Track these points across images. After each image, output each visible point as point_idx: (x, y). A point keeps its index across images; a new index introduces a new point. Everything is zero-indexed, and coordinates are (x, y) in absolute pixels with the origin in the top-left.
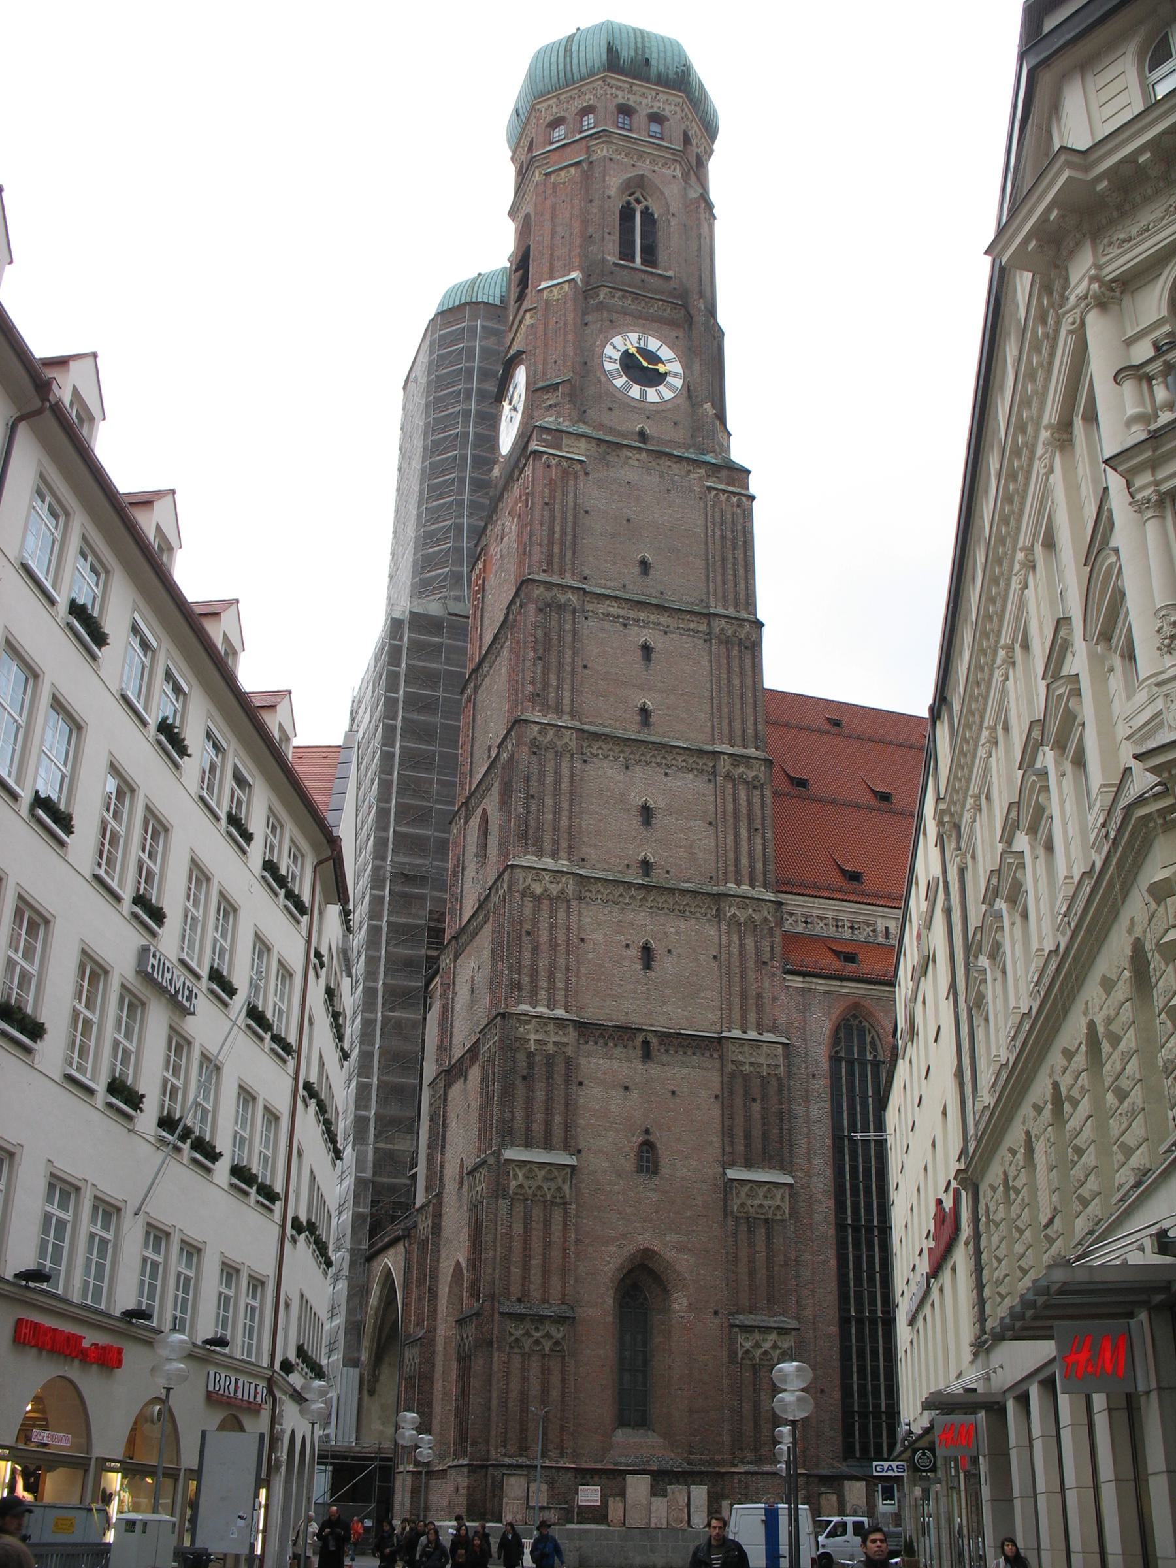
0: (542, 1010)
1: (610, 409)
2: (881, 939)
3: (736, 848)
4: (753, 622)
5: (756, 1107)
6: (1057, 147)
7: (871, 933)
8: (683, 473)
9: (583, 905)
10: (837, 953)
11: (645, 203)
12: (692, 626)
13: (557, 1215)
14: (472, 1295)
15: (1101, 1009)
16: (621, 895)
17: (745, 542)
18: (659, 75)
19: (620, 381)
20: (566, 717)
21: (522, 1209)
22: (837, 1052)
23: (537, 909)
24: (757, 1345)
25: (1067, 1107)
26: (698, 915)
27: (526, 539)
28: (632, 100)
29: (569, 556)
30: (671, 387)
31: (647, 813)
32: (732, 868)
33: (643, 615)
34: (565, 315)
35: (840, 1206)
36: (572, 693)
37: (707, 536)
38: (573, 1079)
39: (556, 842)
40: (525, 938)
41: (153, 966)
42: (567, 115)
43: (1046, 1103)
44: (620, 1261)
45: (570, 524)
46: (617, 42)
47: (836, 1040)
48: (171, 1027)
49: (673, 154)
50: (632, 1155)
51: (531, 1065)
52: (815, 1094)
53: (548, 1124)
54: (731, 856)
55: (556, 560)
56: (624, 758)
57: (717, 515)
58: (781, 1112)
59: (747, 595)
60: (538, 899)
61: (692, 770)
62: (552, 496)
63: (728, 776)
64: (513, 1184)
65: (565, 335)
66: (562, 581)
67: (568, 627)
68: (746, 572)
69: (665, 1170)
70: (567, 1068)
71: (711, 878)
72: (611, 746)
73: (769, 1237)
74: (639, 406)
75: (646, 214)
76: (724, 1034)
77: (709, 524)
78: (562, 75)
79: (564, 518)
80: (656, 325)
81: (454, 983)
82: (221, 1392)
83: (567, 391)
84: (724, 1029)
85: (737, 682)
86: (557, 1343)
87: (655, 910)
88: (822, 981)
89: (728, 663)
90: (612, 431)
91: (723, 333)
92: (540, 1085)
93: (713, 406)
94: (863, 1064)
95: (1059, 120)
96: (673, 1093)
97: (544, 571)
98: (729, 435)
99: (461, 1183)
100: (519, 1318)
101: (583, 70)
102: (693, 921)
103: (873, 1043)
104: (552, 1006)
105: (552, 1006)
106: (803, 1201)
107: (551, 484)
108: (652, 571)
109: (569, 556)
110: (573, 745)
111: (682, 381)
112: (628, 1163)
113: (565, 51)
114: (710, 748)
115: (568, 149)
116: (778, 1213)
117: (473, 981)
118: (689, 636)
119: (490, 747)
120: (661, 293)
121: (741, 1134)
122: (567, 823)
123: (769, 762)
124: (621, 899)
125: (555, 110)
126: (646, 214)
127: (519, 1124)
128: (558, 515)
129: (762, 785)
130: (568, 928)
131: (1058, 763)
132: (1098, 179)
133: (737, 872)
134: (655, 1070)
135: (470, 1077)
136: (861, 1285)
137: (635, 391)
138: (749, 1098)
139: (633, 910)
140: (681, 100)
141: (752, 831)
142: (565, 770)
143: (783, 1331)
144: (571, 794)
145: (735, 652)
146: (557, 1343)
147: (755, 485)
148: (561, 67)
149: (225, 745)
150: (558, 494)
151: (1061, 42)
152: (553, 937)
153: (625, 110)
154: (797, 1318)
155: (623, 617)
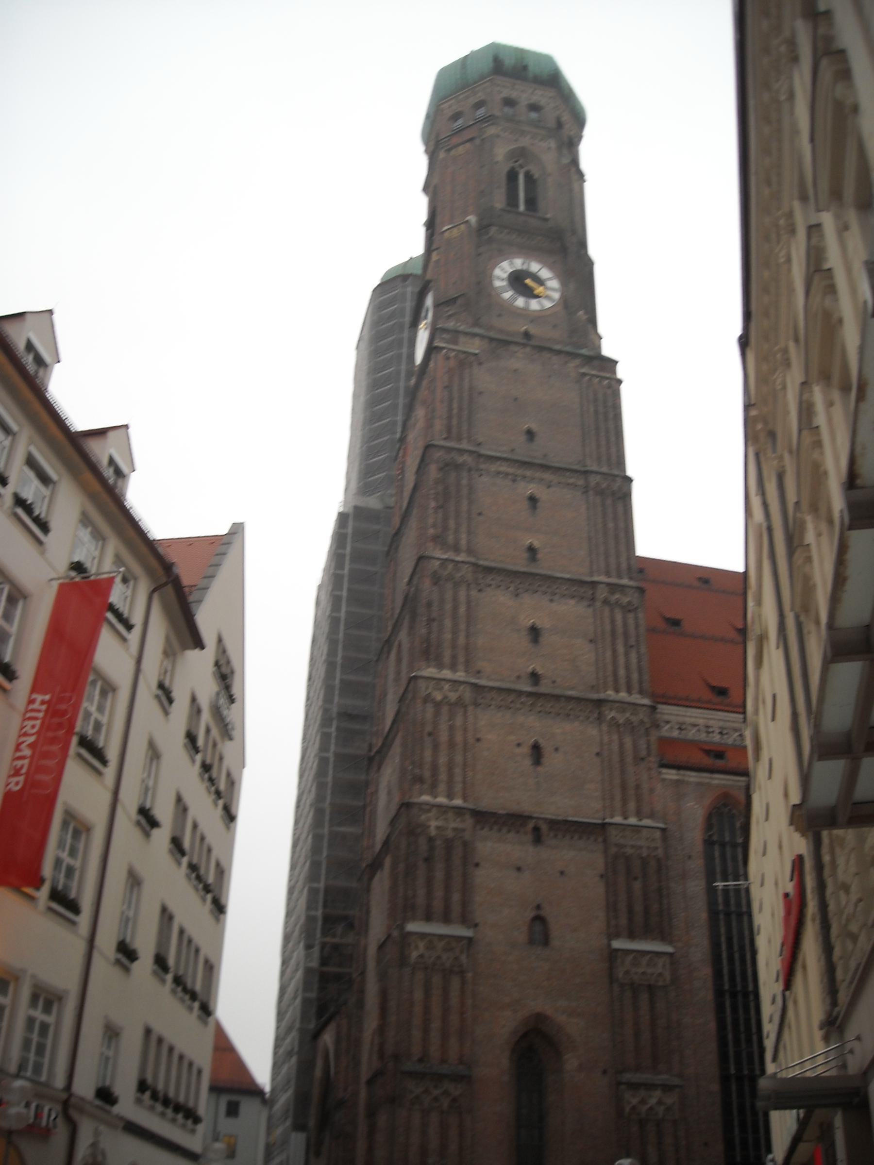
0: (442, 800)
5: (637, 885)
10: (708, 752)
12: (571, 481)
13: (455, 982)
19: (507, 295)
22: (710, 836)
23: (437, 714)
28: (514, 95)
31: (535, 633)
32: (610, 679)
35: (718, 974)
38: (469, 861)
39: (454, 657)
47: (709, 825)
51: (432, 848)
53: (447, 900)
60: (438, 705)
61: (573, 597)
63: (606, 602)
64: (414, 954)
66: (457, 446)
74: (524, 314)
75: (529, 177)
76: (607, 821)
85: (611, 525)
86: (454, 1100)
93: (586, 313)
97: (445, 439)
104: (450, 796)
114: (588, 579)
123: (641, 590)
124: (512, 705)
126: (529, 177)
127: (421, 900)
129: (636, 609)
130: (465, 730)
137: (520, 302)
141: (628, 647)
143: (667, 1088)
145: (609, 502)
146: (454, 1100)
153: (509, 102)
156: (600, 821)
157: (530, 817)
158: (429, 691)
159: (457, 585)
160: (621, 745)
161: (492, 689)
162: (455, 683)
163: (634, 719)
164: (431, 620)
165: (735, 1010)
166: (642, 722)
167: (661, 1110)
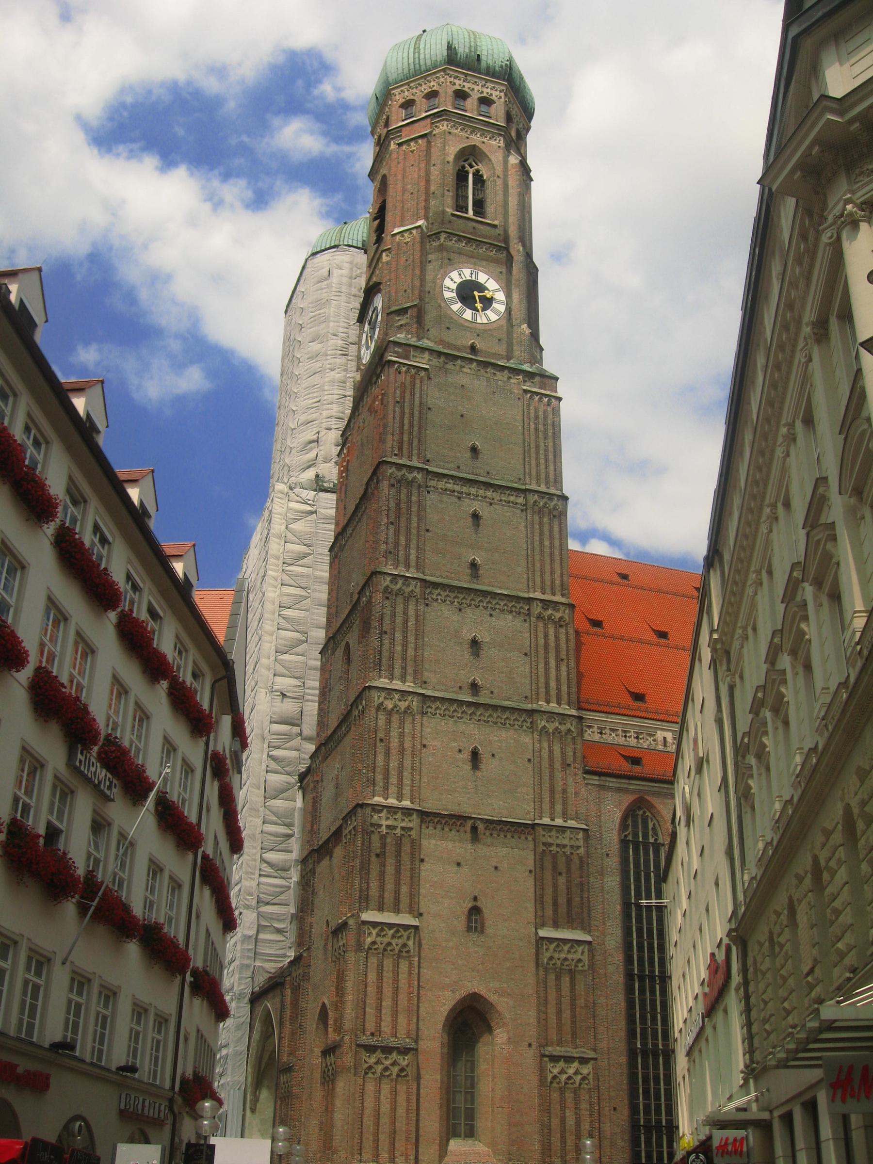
0: (392, 801)
1: (448, 328)
3: (546, 674)
4: (558, 496)
5: (562, 880)
6: (816, 97)
8: (505, 379)
9: (425, 719)
10: (626, 758)
11: (476, 167)
12: (512, 498)
13: (404, 966)
14: (335, 1030)
15: (856, 794)
16: (455, 711)
17: (554, 433)
18: (488, 68)
19: (457, 307)
20: (412, 570)
22: (626, 836)
23: (389, 722)
24: (562, 1072)
25: (826, 876)
26: (516, 727)
27: (381, 430)
29: (415, 443)
30: (496, 312)
31: (475, 644)
32: (542, 690)
34: (413, 254)
35: (629, 960)
36: (417, 552)
39: (404, 668)
40: (379, 744)
41: (81, 761)
42: (415, 98)
43: (806, 873)
44: (453, 1003)
45: (416, 418)
46: (455, 42)
47: (623, 825)
48: (95, 811)
49: (498, 129)
50: (463, 918)
51: (384, 846)
54: (542, 680)
55: (405, 446)
57: (532, 412)
58: (581, 884)
59: (555, 475)
60: (390, 713)
62: (403, 397)
63: (539, 617)
65: (413, 270)
66: (409, 463)
67: (414, 499)
68: (555, 457)
69: (490, 930)
70: (412, 847)
71: (526, 697)
72: (447, 593)
76: (537, 821)
77: (526, 419)
78: (412, 67)
79: (412, 414)
80: (484, 263)
81: (322, 780)
82: (131, 1109)
85: (547, 543)
86: (402, 1070)
87: (482, 722)
88: (615, 780)
90: (449, 345)
91: (537, 270)
93: (529, 327)
94: (646, 845)
95: (817, 78)
96: (496, 868)
97: (396, 455)
98: (542, 349)
99: (327, 939)
100: (371, 1049)
101: (429, 63)
102: (512, 732)
103: (654, 829)
104: (400, 798)
105: (400, 798)
108: (480, 456)
109: (415, 443)
112: (460, 924)
113: (415, 49)
114: (526, 595)
115: (417, 125)
116: (580, 965)
117: (337, 778)
118: (509, 506)
119: (352, 594)
120: (489, 238)
124: (455, 714)
125: (406, 93)
128: (407, 411)
130: (413, 737)
131: (816, 597)
132: (851, 121)
133: (547, 693)
134: (482, 850)
135: (335, 855)
136: (646, 1024)
137: (468, 314)
138: (556, 872)
139: (465, 723)
141: (559, 660)
142: (411, 612)
143: (583, 1061)
144: (416, 630)
145: (546, 520)
146: (402, 1070)
148: (411, 60)
149: (141, 585)
151: (820, 14)
152: (402, 743)
153: (461, 95)
154: (595, 1050)
155: (458, 492)
156: (530, 822)
157: (470, 818)
158: (381, 699)
159: (407, 600)
160: (551, 751)
161: (436, 699)
162: (404, 693)
163: (563, 728)
165: (642, 991)
166: (569, 730)
167: (578, 1078)
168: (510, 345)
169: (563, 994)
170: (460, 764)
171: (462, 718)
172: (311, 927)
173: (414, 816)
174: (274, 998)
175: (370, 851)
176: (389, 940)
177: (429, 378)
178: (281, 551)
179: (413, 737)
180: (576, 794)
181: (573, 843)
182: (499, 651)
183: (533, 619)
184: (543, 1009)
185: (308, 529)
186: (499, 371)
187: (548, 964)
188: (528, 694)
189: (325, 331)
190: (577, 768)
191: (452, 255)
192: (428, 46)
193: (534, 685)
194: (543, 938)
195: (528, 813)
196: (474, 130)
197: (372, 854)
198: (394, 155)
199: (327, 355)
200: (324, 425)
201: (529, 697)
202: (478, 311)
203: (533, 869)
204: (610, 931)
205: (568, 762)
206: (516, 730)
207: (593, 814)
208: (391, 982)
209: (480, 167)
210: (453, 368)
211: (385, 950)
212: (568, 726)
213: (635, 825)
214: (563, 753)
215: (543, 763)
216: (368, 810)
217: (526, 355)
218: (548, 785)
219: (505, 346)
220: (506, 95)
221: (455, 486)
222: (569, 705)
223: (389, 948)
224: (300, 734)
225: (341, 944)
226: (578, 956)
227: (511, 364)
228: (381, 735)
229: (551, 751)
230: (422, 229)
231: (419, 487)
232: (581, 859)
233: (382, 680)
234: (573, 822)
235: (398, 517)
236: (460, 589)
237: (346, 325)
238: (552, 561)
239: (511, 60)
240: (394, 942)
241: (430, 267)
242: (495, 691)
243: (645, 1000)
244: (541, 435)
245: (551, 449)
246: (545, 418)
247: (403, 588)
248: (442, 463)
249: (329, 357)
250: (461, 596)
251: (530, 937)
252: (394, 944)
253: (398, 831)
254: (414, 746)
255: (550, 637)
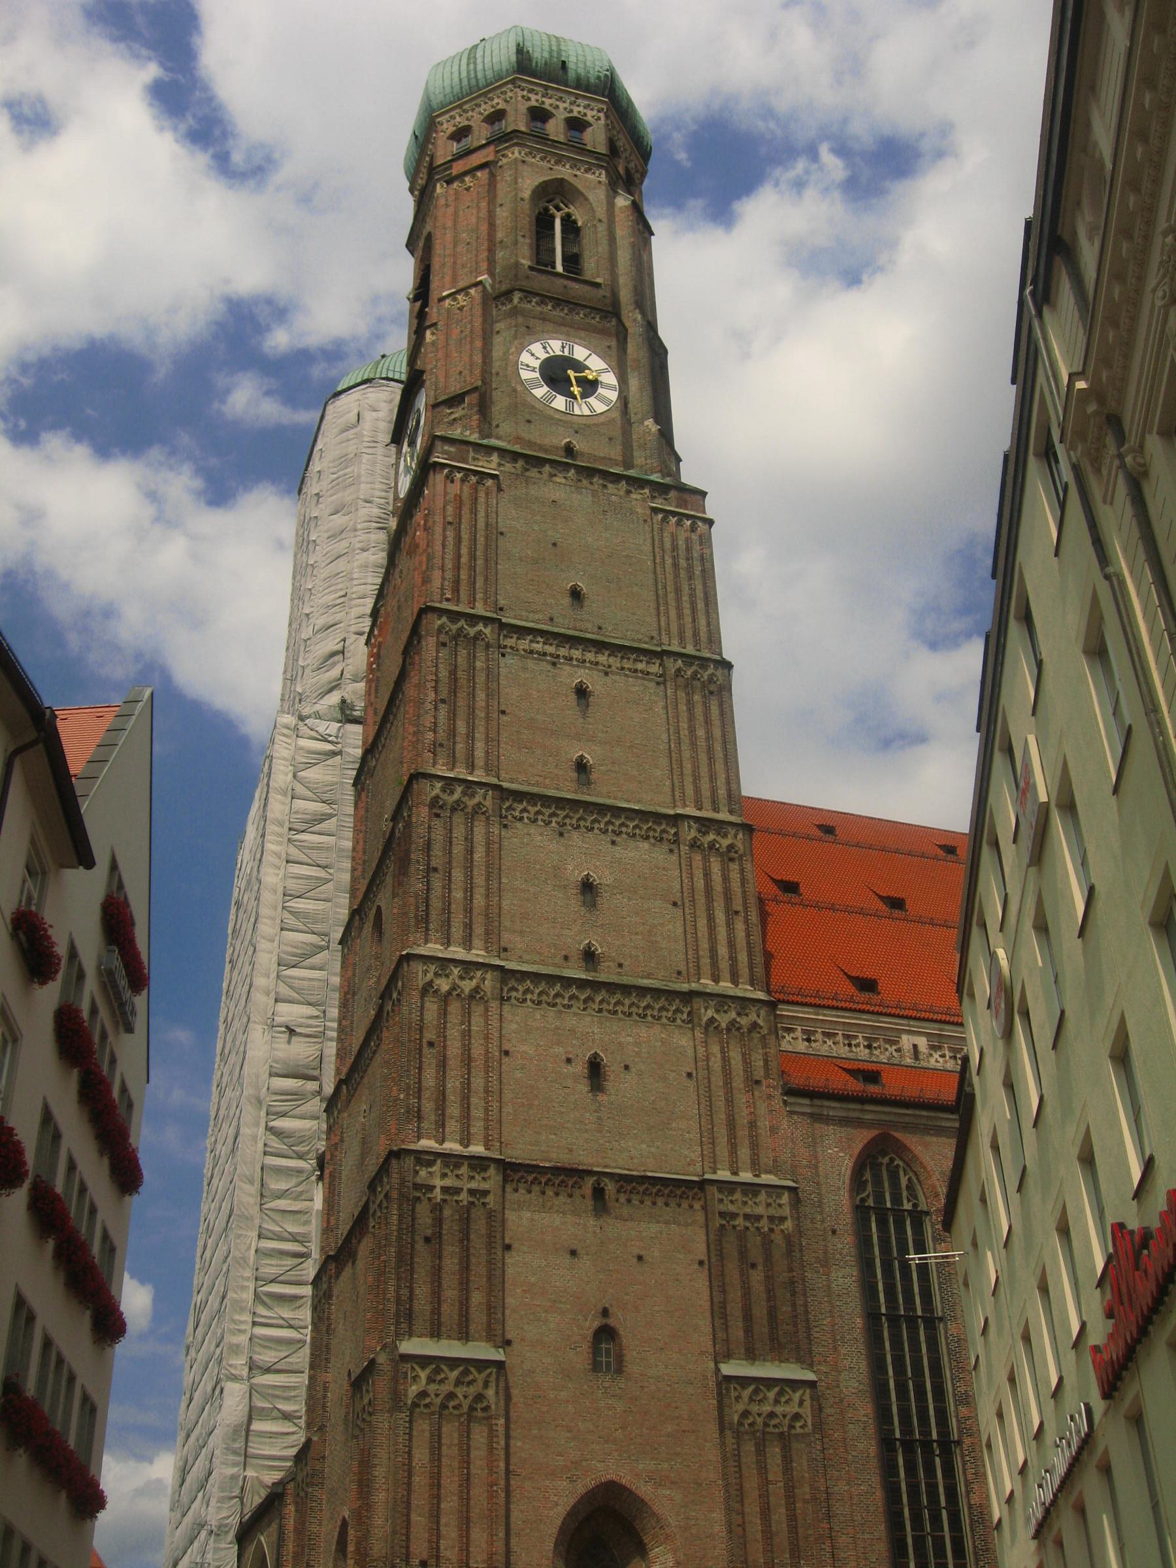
0: (451, 1146)
1: (529, 421)
2: (909, 1060)
3: (710, 935)
4: (715, 661)
7: (895, 1054)
8: (622, 493)
9: (506, 1008)
11: (566, 210)
12: (640, 666)
13: (479, 1435)
16: (557, 995)
17: (703, 571)
18: (578, 78)
19: (541, 391)
21: (426, 1427)
22: (863, 1200)
23: (444, 1013)
26: (664, 1020)
29: (480, 583)
32: (706, 961)
33: (577, 652)
34: (471, 322)
35: (883, 1414)
36: (487, 743)
37: (655, 563)
39: (469, 927)
40: (426, 1050)
44: (572, 1501)
47: (857, 1183)
49: (597, 159)
50: (585, 1348)
51: (439, 1221)
52: (838, 1256)
54: (705, 945)
56: (558, 823)
58: (792, 1282)
59: (709, 631)
60: (446, 998)
61: (647, 838)
63: (694, 845)
65: (471, 343)
67: (478, 664)
68: (707, 605)
69: (633, 1367)
71: (679, 973)
73: (787, 1459)
74: (565, 420)
75: (568, 222)
76: (707, 1176)
77: (657, 550)
78: (465, 82)
80: (583, 334)
81: (342, 1141)
83: (475, 401)
84: (707, 1168)
85: (701, 733)
87: (605, 1014)
89: (689, 710)
90: (530, 444)
91: (666, 352)
92: (451, 1251)
93: (657, 422)
96: (640, 1258)
97: (448, 600)
98: (678, 460)
101: (489, 74)
102: (657, 1030)
104: (466, 1141)
105: (466, 1141)
106: (831, 1406)
107: (455, 500)
108: (586, 604)
110: (488, 803)
111: (617, 393)
112: (580, 1358)
113: (469, 59)
114: (672, 812)
116: (798, 1424)
118: (637, 677)
121: (738, 1314)
122: (483, 903)
124: (558, 1000)
125: (458, 119)
126: (568, 222)
128: (465, 536)
130: (487, 1038)
134: (613, 1227)
136: (922, 1529)
137: (560, 402)
139: (575, 1014)
140: (605, 107)
141: (731, 914)
145: (697, 698)
147: (711, 509)
148: (464, 74)
150: (466, 512)
152: (467, 1049)
155: (551, 655)
156: (695, 1178)
157: (590, 1173)
158: (430, 976)
160: (726, 1060)
161: (524, 975)
162: (468, 967)
164: (431, 870)
165: (911, 1469)
166: (754, 1026)
168: (627, 446)
169: (771, 1477)
170: (569, 1083)
171: (570, 1007)
172: (326, 1389)
173: (492, 1171)
174: (269, 1525)
175: (413, 1232)
176: (451, 1388)
177: (500, 489)
178: (287, 811)
179: (487, 1038)
180: (773, 1130)
181: (772, 1211)
182: (630, 899)
183: (684, 849)
184: (737, 1506)
185: (329, 778)
186: (612, 482)
187: (740, 1424)
188: (683, 968)
189: (353, 496)
190: (772, 1088)
191: (532, 322)
192: (488, 53)
193: (690, 952)
194: (729, 1379)
195: (692, 1163)
196: (560, 160)
197: (417, 1238)
198: (442, 201)
199: (356, 530)
200: (353, 629)
201: (684, 973)
202: (575, 397)
203: (705, 1258)
204: (847, 1363)
205: (758, 1078)
206: (664, 1025)
207: (804, 1162)
208: (456, 1464)
209: (572, 209)
210: (538, 476)
211: (444, 1406)
212: (753, 1017)
213: (878, 1182)
214: (747, 1062)
215: (713, 1079)
216: (409, 1162)
217: (654, 462)
218: (723, 1116)
219: (619, 448)
220: (607, 117)
221: (547, 647)
222: (752, 985)
223: (452, 1404)
224: (319, 1093)
225: (366, 1401)
226: (793, 1408)
227: (631, 473)
228: (429, 1035)
229: (726, 1060)
230: (484, 287)
231: (488, 646)
232: (788, 1238)
233: (429, 945)
234: (772, 1177)
235: (454, 691)
236: (560, 802)
237: (384, 487)
238: (711, 759)
239: (611, 70)
240: (460, 1391)
241: (497, 340)
242: (626, 963)
243: (918, 1486)
244: (683, 574)
245: (700, 594)
246: (689, 549)
247: (465, 799)
248: (524, 613)
249: (358, 533)
250: (562, 813)
251: (705, 1378)
252: (460, 1396)
253: (464, 1197)
254: (487, 1053)
255: (714, 877)
